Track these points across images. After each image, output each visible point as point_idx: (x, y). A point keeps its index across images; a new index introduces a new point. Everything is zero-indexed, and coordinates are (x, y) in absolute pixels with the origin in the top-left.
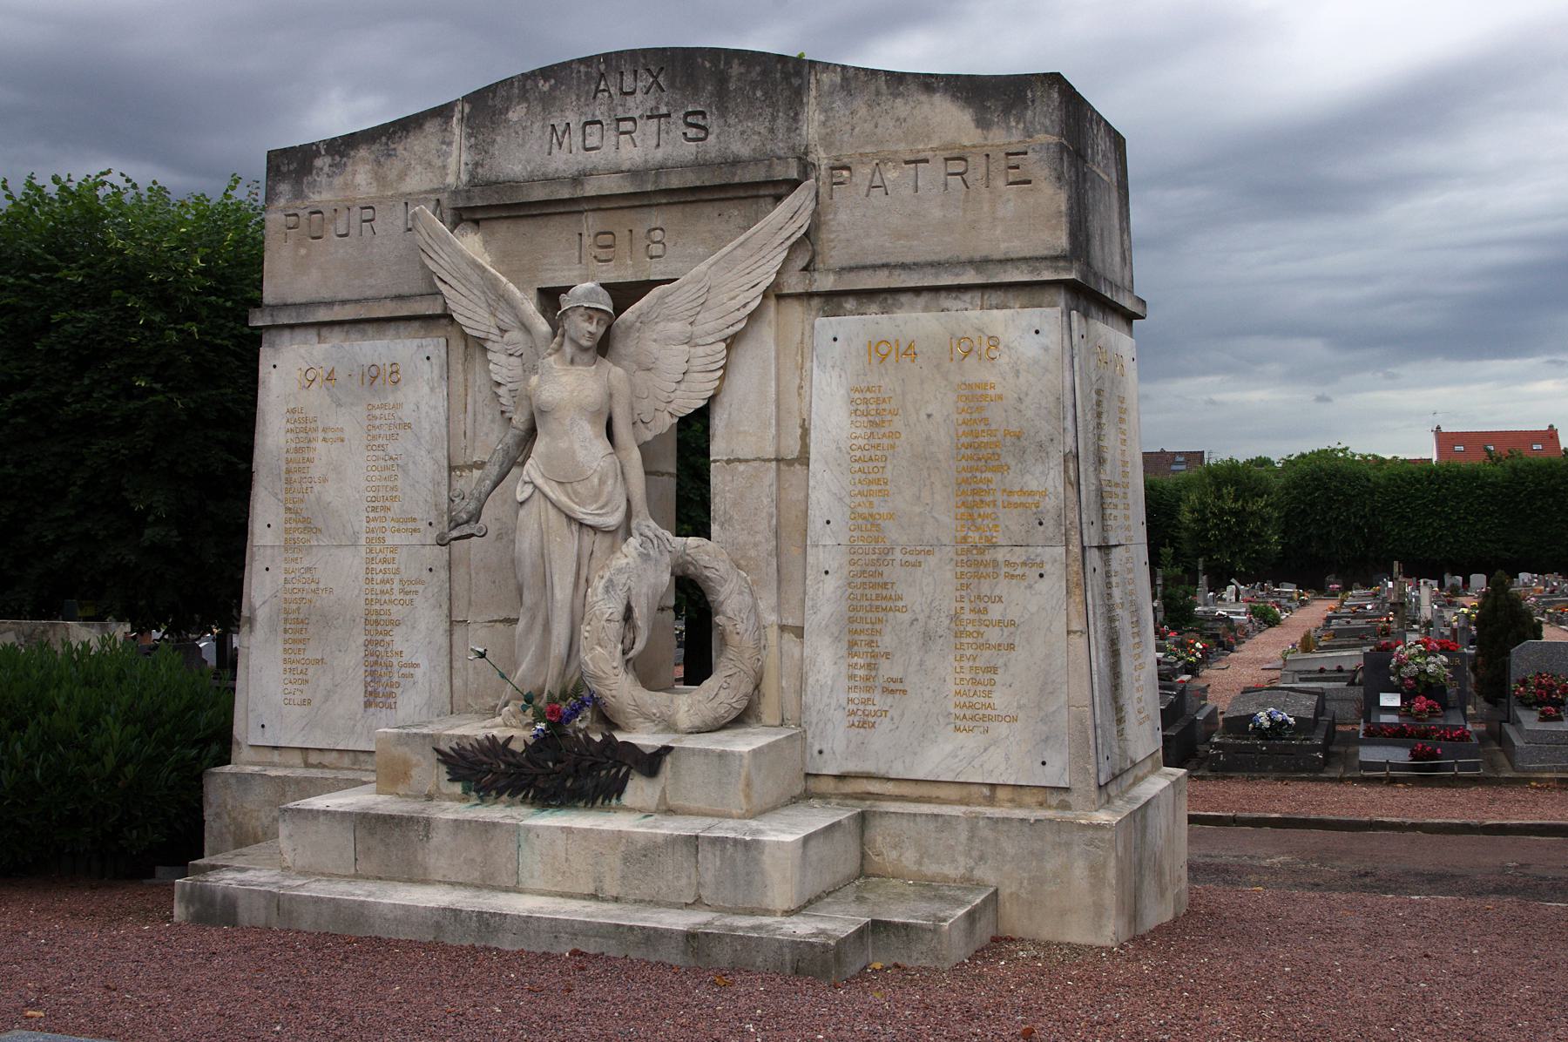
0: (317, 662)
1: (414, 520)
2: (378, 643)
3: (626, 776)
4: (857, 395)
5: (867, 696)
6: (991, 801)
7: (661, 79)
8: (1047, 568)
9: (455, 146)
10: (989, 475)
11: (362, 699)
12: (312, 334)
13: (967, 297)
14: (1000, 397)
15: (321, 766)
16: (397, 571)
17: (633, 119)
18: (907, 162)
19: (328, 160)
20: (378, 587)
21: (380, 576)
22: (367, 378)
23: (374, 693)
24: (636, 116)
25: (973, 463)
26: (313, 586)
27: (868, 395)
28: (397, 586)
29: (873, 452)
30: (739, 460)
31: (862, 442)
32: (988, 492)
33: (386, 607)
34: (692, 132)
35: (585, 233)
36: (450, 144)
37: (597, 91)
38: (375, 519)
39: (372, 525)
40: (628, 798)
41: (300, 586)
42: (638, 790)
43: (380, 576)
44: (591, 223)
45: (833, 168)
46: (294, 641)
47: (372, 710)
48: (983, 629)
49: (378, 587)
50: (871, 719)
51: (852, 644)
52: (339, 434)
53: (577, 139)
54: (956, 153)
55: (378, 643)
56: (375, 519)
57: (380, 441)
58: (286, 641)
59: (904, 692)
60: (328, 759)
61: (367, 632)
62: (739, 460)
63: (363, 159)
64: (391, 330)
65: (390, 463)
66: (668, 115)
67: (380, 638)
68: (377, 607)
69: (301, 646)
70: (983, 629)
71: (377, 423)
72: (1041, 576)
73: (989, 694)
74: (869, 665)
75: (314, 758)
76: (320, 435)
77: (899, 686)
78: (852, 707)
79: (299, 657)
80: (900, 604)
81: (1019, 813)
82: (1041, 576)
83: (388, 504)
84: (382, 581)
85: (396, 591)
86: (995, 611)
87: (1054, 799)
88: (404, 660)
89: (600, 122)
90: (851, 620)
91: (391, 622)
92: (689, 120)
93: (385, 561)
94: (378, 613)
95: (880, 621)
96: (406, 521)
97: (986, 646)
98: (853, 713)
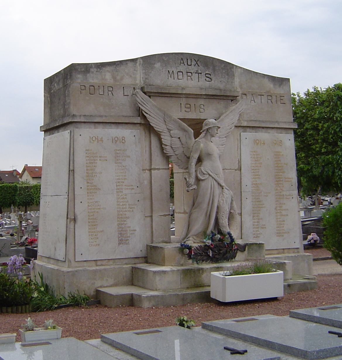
0: (101, 232)
1: (132, 186)
2: (122, 224)
3: (237, 252)
4: (252, 153)
5: (257, 229)
6: (284, 253)
7: (198, 63)
8: (294, 196)
9: (139, 72)
10: (281, 174)
11: (117, 242)
12: (92, 126)
13: (274, 130)
14: (283, 155)
15: (102, 265)
16: (128, 202)
17: (191, 73)
18: (259, 95)
19: (95, 70)
20: (121, 207)
21: (122, 203)
22: (114, 141)
23: (121, 240)
24: (192, 72)
25: (278, 171)
26: (98, 207)
27: (255, 153)
28: (127, 206)
29: (256, 168)
30: (226, 169)
31: (254, 165)
32: (281, 178)
33: (124, 213)
34: (208, 79)
35: (182, 103)
36: (137, 71)
37: (181, 63)
38: (119, 186)
39: (118, 187)
40: (237, 258)
41: (94, 207)
42: (240, 256)
43: (122, 203)
44: (183, 101)
45: (242, 94)
46: (92, 225)
47: (121, 245)
48: (281, 211)
49: (121, 207)
50: (258, 235)
51: (253, 216)
52: (106, 158)
53: (176, 76)
54: (270, 94)
55: (122, 224)
56: (119, 186)
57: (120, 161)
58: (89, 226)
59: (265, 228)
60: (104, 263)
61: (118, 221)
62: (226, 169)
63: (108, 71)
64: (120, 126)
65: (123, 168)
66: (201, 73)
67: (123, 223)
68: (121, 213)
69: (95, 227)
70: (281, 211)
71: (118, 155)
72: (293, 198)
73: (254, 231)
74: (257, 222)
75: (99, 263)
76: (99, 159)
77: (264, 227)
78: (254, 233)
79: (94, 230)
80: (264, 206)
81: (290, 255)
82: (293, 198)
83: (123, 181)
84: (123, 205)
85: (127, 207)
86: (284, 207)
87: (296, 251)
88: (132, 228)
89: (182, 72)
90: (253, 210)
91: (127, 218)
92: (207, 75)
93: (123, 198)
94: (122, 215)
95: (259, 210)
96: (129, 186)
97: (282, 215)
98: (254, 234)
